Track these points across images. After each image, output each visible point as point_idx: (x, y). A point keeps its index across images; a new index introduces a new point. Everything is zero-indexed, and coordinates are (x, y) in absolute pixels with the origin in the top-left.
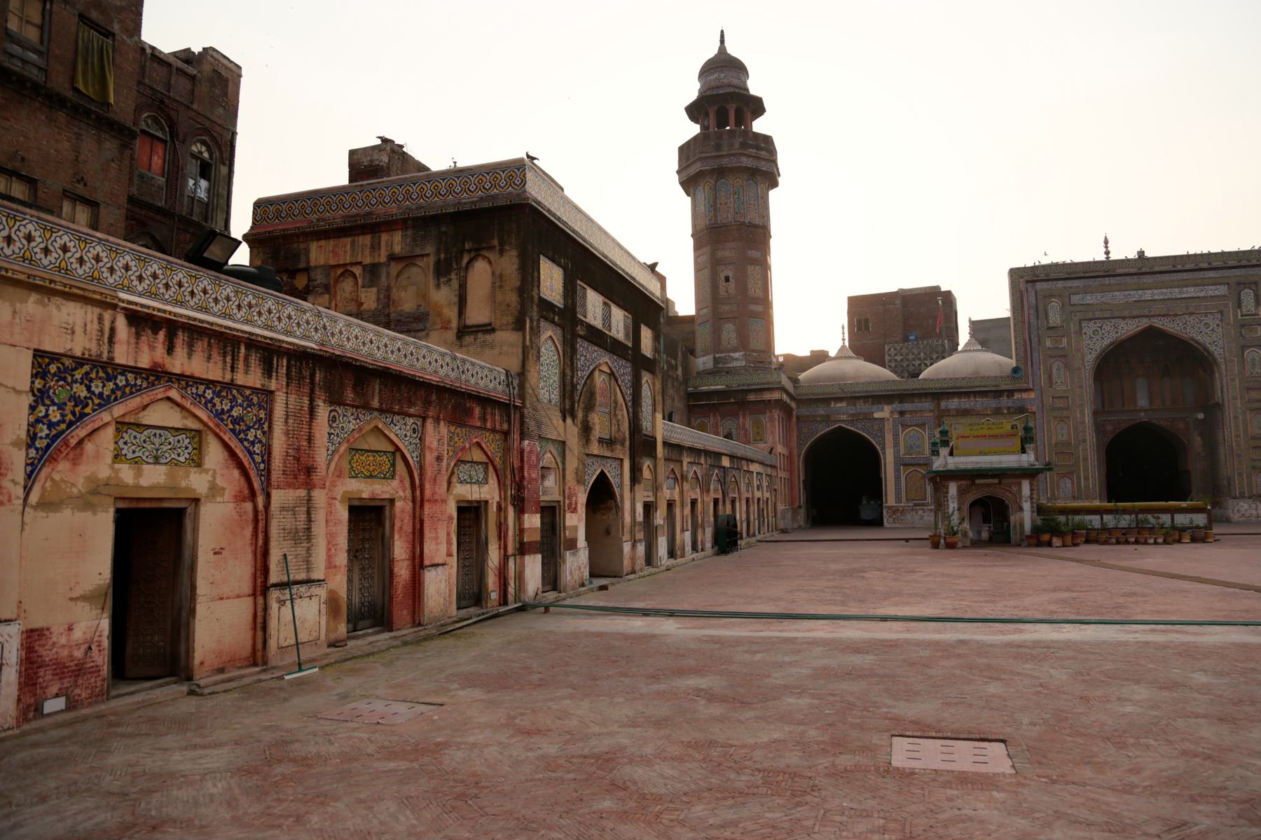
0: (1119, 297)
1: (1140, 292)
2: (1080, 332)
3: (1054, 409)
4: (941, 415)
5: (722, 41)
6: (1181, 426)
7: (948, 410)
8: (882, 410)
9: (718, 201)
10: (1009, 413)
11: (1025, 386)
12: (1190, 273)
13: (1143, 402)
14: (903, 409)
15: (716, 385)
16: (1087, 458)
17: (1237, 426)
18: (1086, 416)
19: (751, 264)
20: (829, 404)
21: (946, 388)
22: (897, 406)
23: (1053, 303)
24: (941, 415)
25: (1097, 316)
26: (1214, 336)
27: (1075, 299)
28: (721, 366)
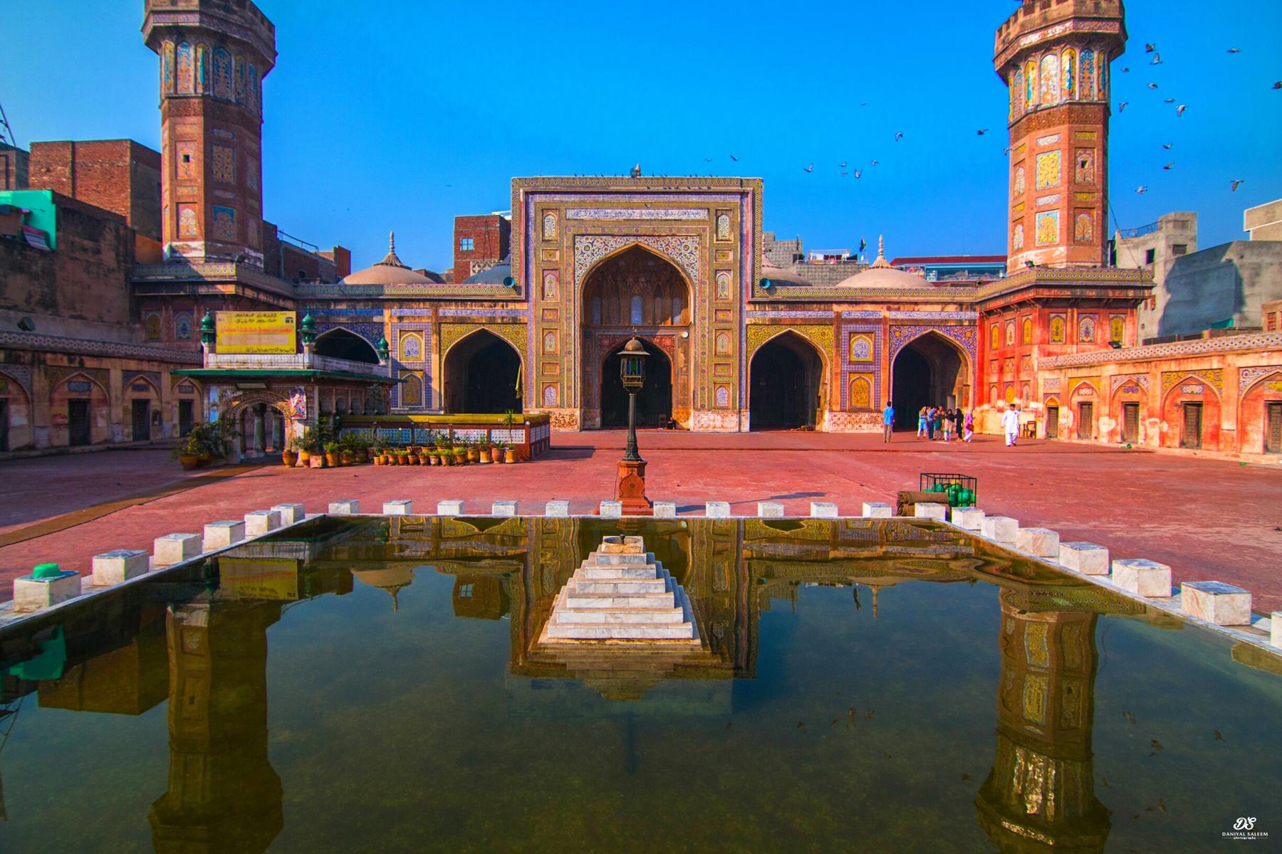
0: (611, 214)
1: (630, 211)
6: (668, 342)
7: (446, 317)
9: (179, 67)
10: (503, 324)
12: (676, 196)
14: (402, 314)
15: (166, 275)
18: (572, 328)
19: (218, 145)
20: (329, 306)
21: (444, 295)
24: (439, 322)
25: (589, 232)
26: (692, 258)
27: (570, 214)
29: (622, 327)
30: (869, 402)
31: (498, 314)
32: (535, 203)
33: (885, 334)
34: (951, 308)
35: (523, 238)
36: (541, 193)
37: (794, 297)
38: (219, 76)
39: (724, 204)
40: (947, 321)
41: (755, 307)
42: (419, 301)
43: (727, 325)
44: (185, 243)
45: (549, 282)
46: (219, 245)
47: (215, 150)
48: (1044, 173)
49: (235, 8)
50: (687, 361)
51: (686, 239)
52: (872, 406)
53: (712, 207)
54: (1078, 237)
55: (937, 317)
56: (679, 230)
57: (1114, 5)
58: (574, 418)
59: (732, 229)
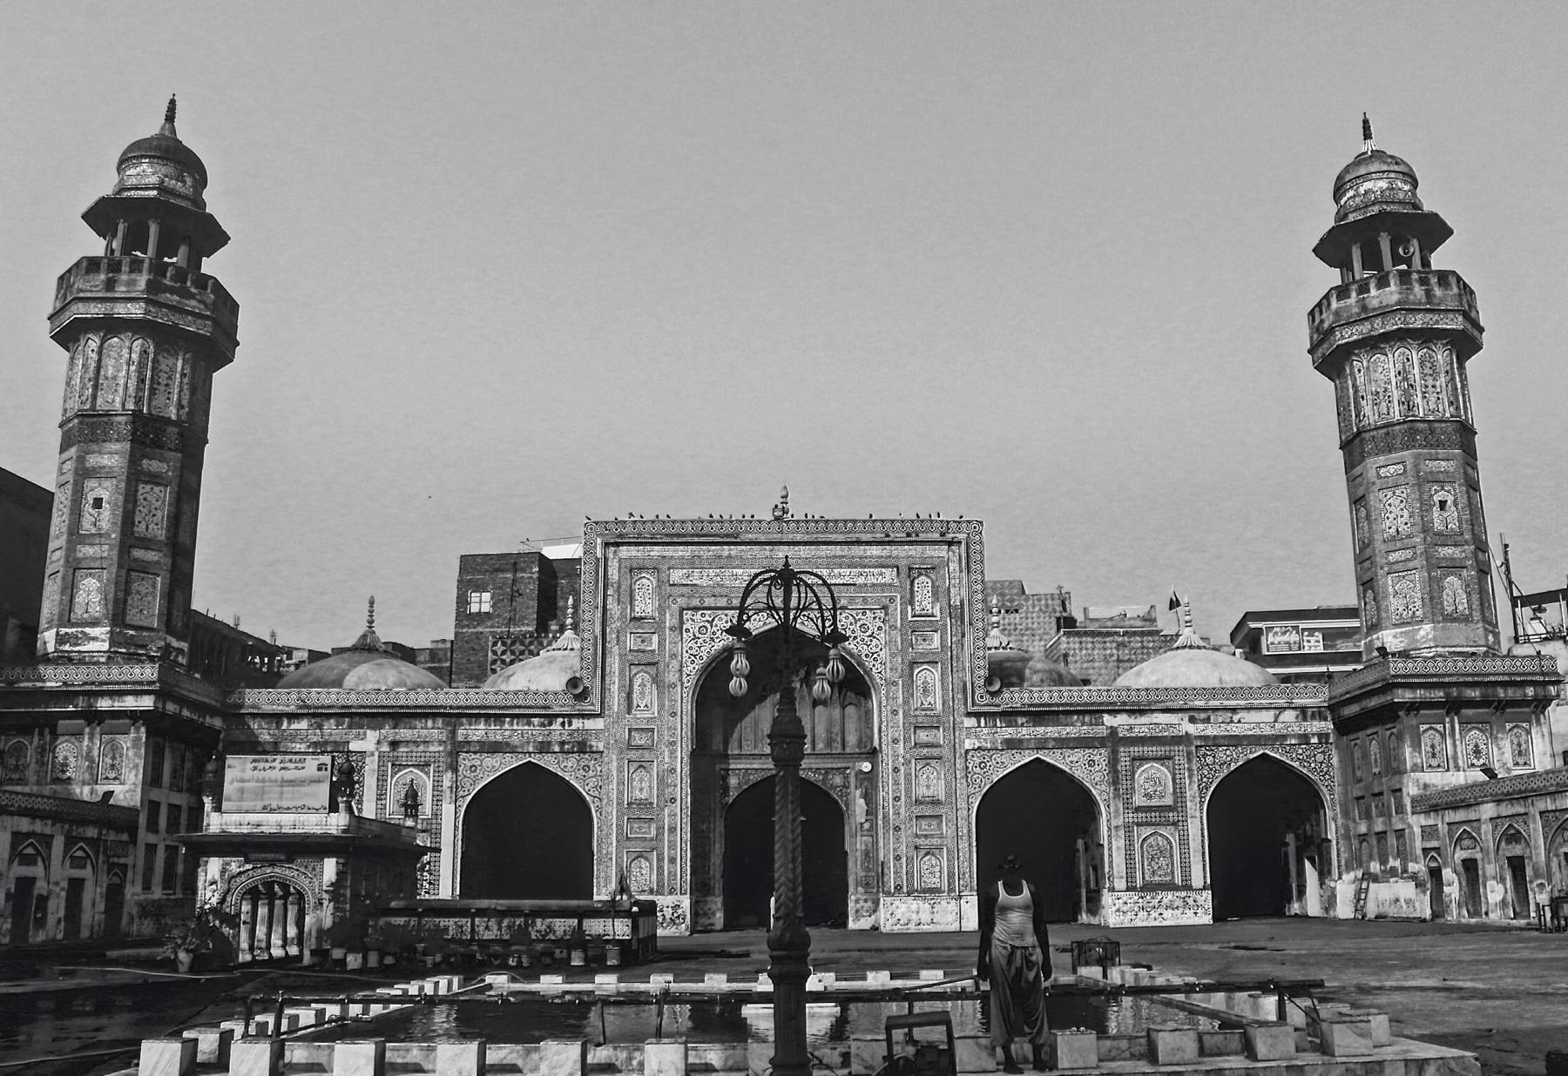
2: (679, 628)
3: (630, 747)
4: (456, 749)
5: (170, 117)
11: (586, 707)
14: (398, 738)
16: (675, 829)
17: (896, 783)
18: (676, 758)
19: (146, 483)
20: (279, 724)
22: (388, 732)
23: (644, 580)
24: (456, 749)
26: (874, 643)
28: (67, 647)
30: (1173, 873)
31: (556, 737)
32: (620, 560)
33: (1190, 761)
34: (1289, 716)
35: (599, 614)
36: (629, 544)
38: (159, 384)
39: (924, 560)
40: (1284, 737)
41: (979, 722)
42: (426, 716)
43: (935, 752)
44: (80, 629)
45: (643, 685)
46: (131, 632)
47: (141, 491)
48: (1392, 516)
49: (193, 290)
50: (871, 812)
53: (903, 563)
54: (1449, 609)
55: (1267, 731)
56: (852, 599)
57: (1451, 293)
58: (680, 911)
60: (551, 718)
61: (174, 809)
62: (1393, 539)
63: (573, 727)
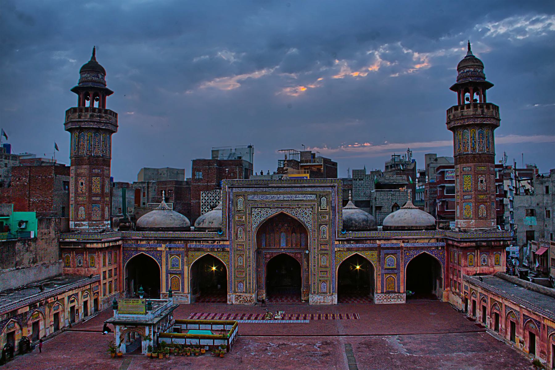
2: (251, 214)
3: (237, 250)
4: (188, 250)
7: (191, 248)
8: (161, 247)
10: (218, 251)
12: (300, 188)
13: (283, 244)
20: (137, 242)
27: (250, 197)
28: (77, 227)
29: (276, 249)
37: (358, 237)
39: (324, 192)
42: (179, 240)
43: (326, 252)
45: (240, 231)
46: (94, 222)
51: (306, 209)
52: (396, 291)
56: (302, 205)
59: (327, 205)
60: (214, 241)
61: (110, 271)
62: (466, 191)
63: (221, 244)
